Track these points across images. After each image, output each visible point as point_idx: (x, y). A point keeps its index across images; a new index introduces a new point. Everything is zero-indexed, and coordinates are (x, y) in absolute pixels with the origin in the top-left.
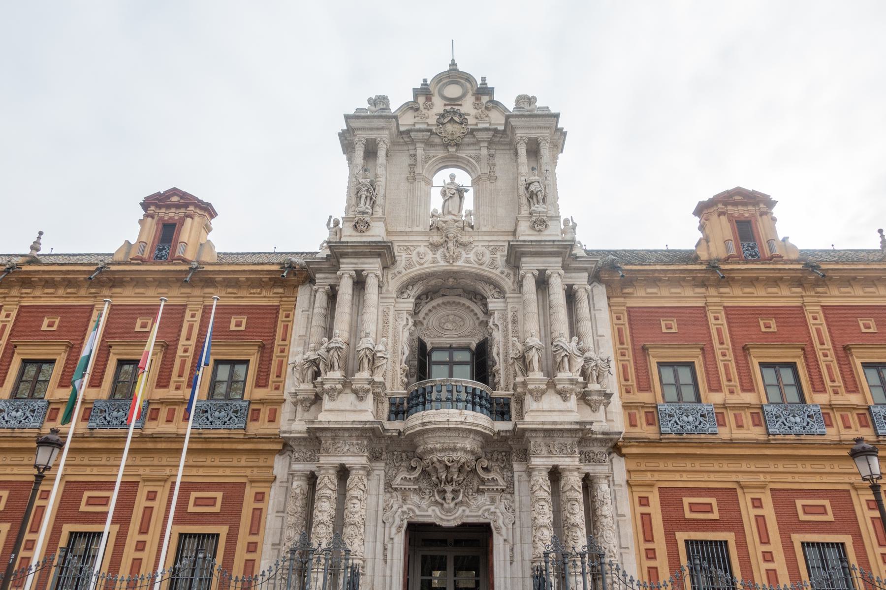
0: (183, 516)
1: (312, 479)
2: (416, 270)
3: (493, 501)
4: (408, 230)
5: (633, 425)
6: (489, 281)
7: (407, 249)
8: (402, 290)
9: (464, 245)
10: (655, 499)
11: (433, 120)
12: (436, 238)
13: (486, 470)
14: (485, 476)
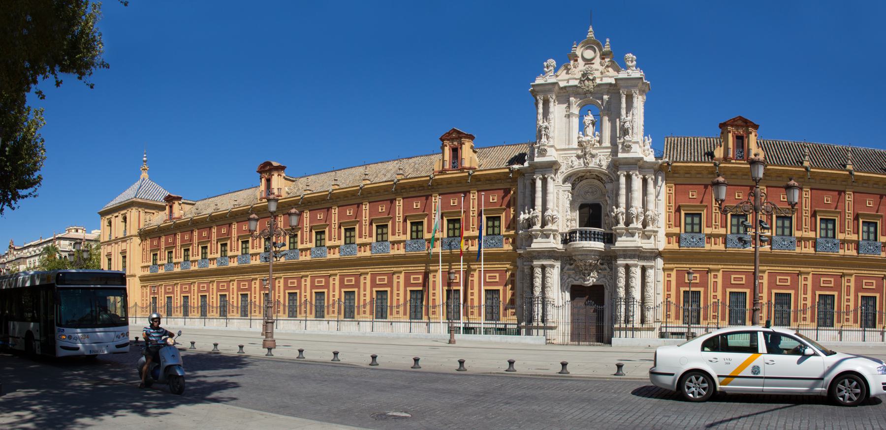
0: (486, 283)
1: (532, 269)
2: (570, 171)
3: (605, 276)
4: (567, 147)
5: (669, 243)
6: (605, 174)
7: (566, 158)
8: (564, 181)
9: (593, 156)
10: (674, 274)
11: (579, 76)
12: (579, 152)
13: (602, 264)
14: (602, 267)
